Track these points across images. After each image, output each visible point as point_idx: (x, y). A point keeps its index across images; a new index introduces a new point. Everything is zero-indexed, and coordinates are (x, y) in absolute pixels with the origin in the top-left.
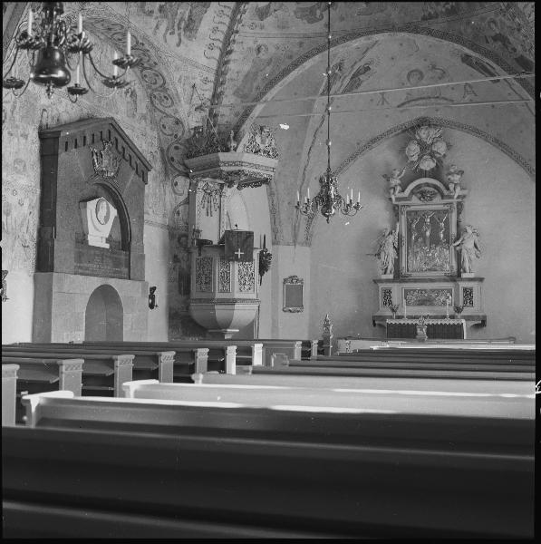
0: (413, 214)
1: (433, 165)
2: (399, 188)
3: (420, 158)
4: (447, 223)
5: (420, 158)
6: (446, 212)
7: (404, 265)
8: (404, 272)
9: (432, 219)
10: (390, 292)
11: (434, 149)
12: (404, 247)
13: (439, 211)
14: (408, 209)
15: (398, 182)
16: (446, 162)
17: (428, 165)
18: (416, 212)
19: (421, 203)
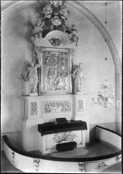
0: (47, 52)
1: (60, 23)
2: (41, 34)
3: (53, 16)
4: (66, 61)
5: (53, 16)
6: (66, 54)
7: (42, 86)
8: (43, 91)
9: (58, 57)
10: (36, 104)
11: (61, 13)
12: (42, 74)
13: (62, 53)
14: (44, 50)
15: (41, 29)
16: (66, 23)
17: (57, 22)
18: (49, 52)
19: (52, 46)
